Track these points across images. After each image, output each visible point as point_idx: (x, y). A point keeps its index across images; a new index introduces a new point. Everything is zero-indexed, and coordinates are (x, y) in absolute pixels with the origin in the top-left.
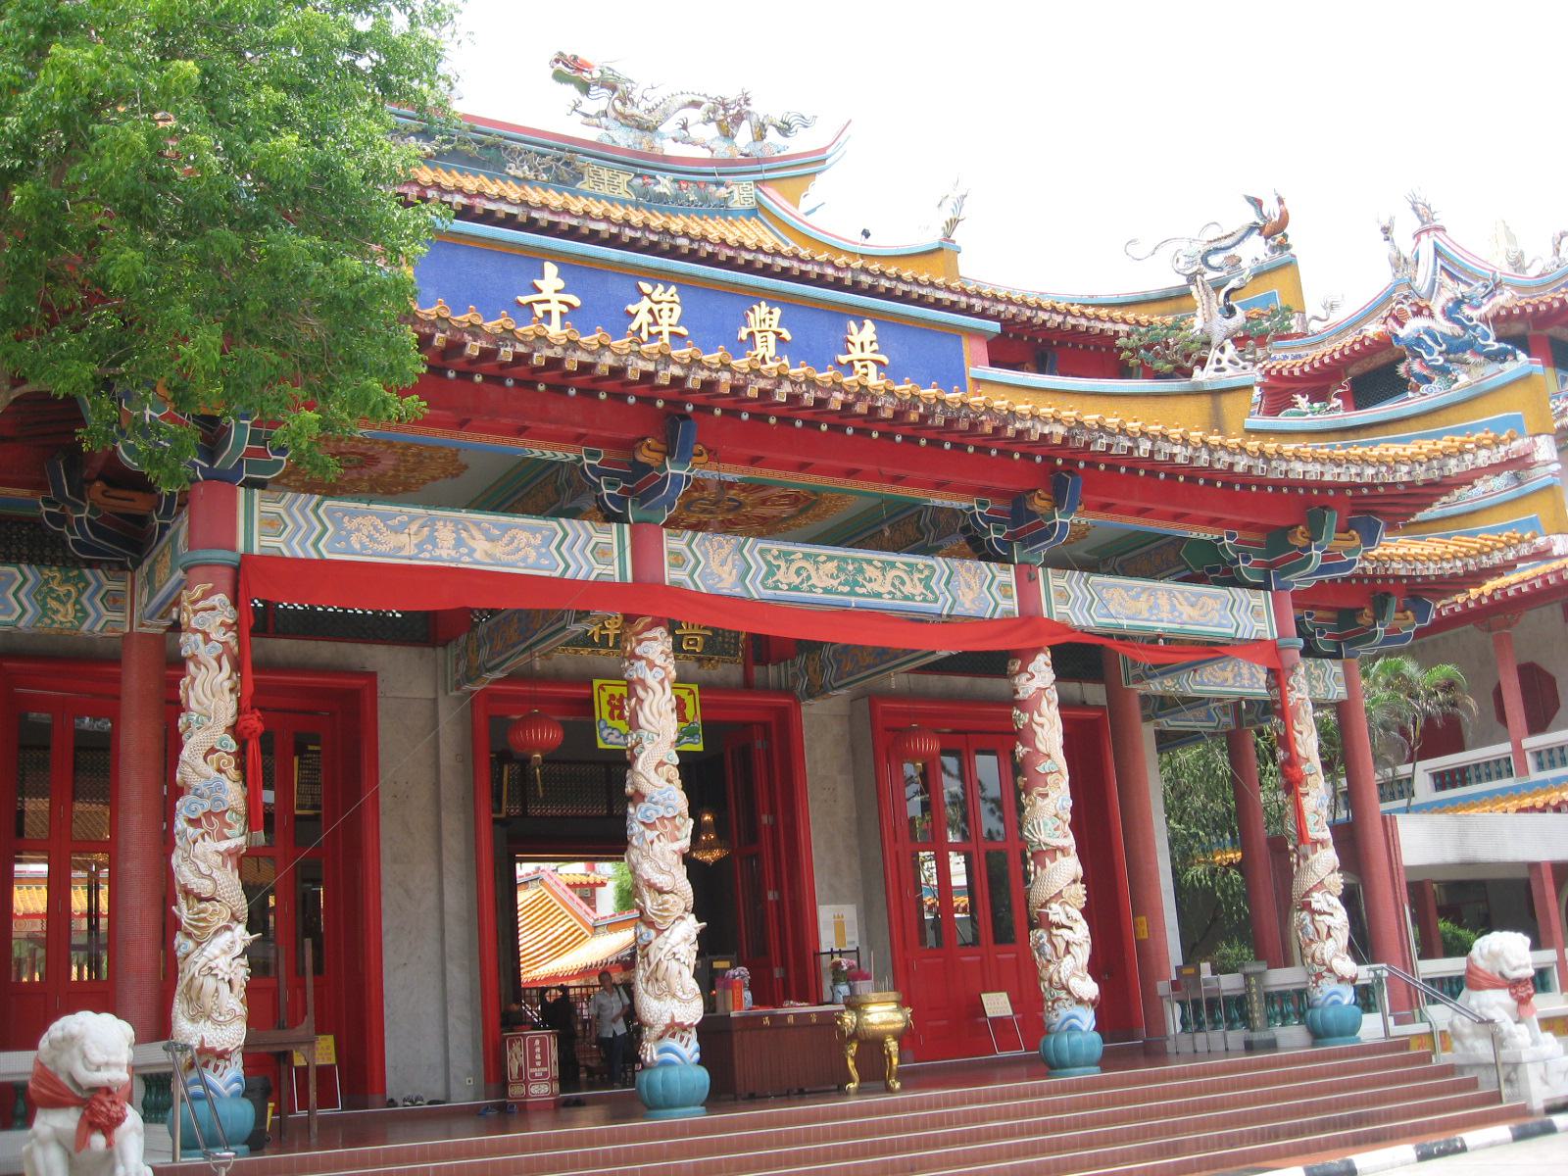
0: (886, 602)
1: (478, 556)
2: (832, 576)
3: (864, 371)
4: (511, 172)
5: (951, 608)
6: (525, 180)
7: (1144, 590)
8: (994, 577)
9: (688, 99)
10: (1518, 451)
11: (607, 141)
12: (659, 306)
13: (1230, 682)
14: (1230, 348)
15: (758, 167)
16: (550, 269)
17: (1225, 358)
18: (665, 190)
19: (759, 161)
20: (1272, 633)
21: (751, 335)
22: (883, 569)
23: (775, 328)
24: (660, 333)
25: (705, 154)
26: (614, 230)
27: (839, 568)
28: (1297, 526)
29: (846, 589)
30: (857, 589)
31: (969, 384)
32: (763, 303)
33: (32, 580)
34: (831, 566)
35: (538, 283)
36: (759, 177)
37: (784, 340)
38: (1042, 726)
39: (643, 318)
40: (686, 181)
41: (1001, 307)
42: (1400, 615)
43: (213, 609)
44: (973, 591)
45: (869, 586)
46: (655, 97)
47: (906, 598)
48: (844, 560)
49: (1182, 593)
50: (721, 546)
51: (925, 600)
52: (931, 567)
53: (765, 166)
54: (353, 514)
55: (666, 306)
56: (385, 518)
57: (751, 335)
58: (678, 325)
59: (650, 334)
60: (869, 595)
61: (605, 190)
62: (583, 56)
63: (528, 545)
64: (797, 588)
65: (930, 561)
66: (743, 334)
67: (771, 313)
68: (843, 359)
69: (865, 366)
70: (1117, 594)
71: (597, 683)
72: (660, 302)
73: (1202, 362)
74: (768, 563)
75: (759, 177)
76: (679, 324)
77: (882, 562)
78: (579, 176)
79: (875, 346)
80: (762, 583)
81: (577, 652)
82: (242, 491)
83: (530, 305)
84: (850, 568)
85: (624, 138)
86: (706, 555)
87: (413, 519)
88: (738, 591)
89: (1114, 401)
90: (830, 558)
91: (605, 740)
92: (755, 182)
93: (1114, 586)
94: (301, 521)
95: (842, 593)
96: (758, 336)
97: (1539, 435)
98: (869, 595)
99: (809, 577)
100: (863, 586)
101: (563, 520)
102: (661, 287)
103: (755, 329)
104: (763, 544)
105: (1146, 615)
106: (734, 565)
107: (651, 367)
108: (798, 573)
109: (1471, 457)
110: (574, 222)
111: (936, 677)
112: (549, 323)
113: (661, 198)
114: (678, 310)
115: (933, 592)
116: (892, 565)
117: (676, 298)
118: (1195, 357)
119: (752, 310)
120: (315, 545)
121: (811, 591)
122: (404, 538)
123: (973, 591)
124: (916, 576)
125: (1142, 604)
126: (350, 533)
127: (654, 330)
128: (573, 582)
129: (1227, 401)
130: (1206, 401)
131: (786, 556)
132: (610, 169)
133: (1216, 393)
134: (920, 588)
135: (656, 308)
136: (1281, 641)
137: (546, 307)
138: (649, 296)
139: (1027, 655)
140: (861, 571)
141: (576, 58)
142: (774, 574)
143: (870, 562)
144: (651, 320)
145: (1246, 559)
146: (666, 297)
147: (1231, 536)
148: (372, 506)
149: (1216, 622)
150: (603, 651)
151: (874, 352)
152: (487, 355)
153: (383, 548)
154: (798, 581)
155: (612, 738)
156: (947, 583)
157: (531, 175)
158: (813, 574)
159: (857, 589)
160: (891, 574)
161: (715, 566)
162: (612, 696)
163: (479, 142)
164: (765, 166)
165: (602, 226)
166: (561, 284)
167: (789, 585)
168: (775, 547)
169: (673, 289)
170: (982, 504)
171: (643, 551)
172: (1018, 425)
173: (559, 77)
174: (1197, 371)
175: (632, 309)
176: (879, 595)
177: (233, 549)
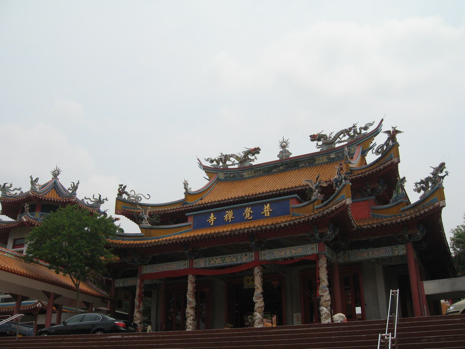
0: (229, 263)
2: (220, 261)
4: (300, 166)
5: (241, 262)
6: (303, 167)
7: (283, 250)
9: (341, 132)
10: (342, 204)
11: (322, 151)
13: (366, 256)
15: (357, 141)
16: (212, 214)
18: (334, 157)
19: (358, 139)
20: (316, 252)
21: (245, 214)
22: (229, 258)
25: (346, 143)
26: (234, 200)
27: (221, 259)
29: (222, 262)
30: (224, 262)
31: (291, 209)
34: (220, 259)
35: (210, 217)
36: (358, 143)
39: (227, 217)
40: (340, 152)
42: (413, 230)
45: (226, 261)
46: (333, 135)
47: (233, 262)
49: (293, 249)
50: (202, 260)
51: (236, 261)
52: (238, 255)
53: (359, 141)
55: (230, 214)
60: (226, 263)
61: (321, 162)
62: (316, 134)
64: (214, 264)
65: (237, 254)
66: (244, 215)
67: (249, 209)
68: (262, 213)
69: (267, 213)
70: (276, 252)
71: (244, 277)
74: (209, 261)
75: (358, 143)
78: (315, 161)
79: (269, 208)
80: (208, 264)
83: (209, 221)
85: (325, 148)
86: (200, 262)
88: (204, 266)
90: (220, 258)
91: (245, 287)
92: (357, 145)
93: (277, 250)
95: (221, 263)
96: (246, 214)
97: (346, 198)
98: (226, 263)
104: (209, 258)
105: (283, 255)
109: (331, 208)
110: (227, 201)
113: (333, 158)
114: (232, 214)
116: (230, 257)
117: (232, 212)
119: (246, 210)
125: (283, 253)
127: (228, 219)
128: (181, 270)
129: (316, 203)
131: (212, 259)
132: (321, 156)
134: (235, 260)
137: (211, 221)
139: (254, 268)
140: (225, 259)
141: (314, 135)
142: (210, 262)
143: (226, 257)
146: (231, 212)
148: (157, 265)
155: (246, 287)
157: (304, 165)
159: (224, 262)
160: (230, 258)
161: (201, 263)
162: (247, 279)
163: (294, 162)
164: (359, 141)
165: (232, 200)
168: (210, 258)
172: (221, 234)
173: (312, 140)
175: (224, 216)
176: (228, 262)
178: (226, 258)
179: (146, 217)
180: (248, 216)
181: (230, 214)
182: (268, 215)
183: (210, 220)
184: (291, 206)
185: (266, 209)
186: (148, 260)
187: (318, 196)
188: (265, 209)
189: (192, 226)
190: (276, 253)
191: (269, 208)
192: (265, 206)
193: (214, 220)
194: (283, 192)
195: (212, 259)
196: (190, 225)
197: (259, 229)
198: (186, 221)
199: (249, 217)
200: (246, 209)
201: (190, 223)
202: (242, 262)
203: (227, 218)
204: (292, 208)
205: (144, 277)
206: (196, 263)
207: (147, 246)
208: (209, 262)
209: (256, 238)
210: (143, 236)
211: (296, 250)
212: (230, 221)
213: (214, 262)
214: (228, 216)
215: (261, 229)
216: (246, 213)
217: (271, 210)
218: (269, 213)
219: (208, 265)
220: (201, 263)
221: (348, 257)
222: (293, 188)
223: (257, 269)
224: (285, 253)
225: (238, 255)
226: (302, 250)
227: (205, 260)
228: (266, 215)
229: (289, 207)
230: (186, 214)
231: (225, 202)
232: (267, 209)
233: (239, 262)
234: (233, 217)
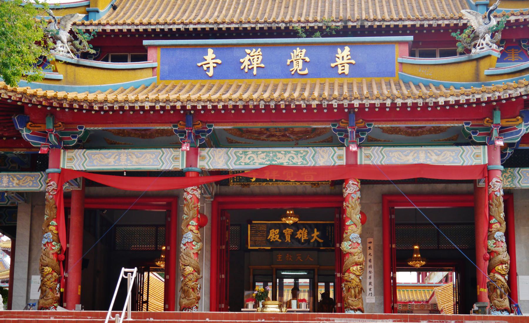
1: (134, 163)
2: (263, 159)
3: (343, 68)
7: (411, 151)
8: (335, 153)
12: (253, 58)
14: (488, 37)
16: (210, 51)
17: (484, 43)
21: (292, 62)
23: (302, 57)
24: (253, 68)
27: (267, 156)
28: (485, 118)
32: (298, 49)
33: (44, 176)
34: (263, 155)
35: (205, 57)
37: (306, 62)
38: (348, 207)
39: (247, 63)
41: (440, 22)
43: (51, 185)
44: (328, 157)
48: (269, 152)
49: (432, 151)
50: (219, 152)
54: (95, 154)
55: (256, 57)
56: (104, 154)
57: (292, 62)
58: (260, 64)
59: (248, 69)
63: (150, 158)
64: (248, 164)
65: (306, 149)
66: (288, 63)
68: (333, 65)
69: (344, 66)
70: (396, 154)
72: (254, 56)
73: (475, 46)
76: (262, 62)
77: (285, 152)
79: (349, 57)
80: (234, 163)
81: (260, 184)
82: (62, 151)
83: (202, 66)
84: (271, 155)
87: (113, 154)
88: (225, 167)
89: (441, 67)
90: (263, 152)
93: (396, 151)
94: (79, 158)
96: (295, 62)
99: (254, 160)
100: (276, 161)
101: (163, 149)
102: (254, 50)
103: (293, 59)
106: (224, 158)
107: (153, 104)
108: (249, 159)
110: (237, 26)
111: (426, 185)
112: (209, 72)
115: (306, 161)
116: (289, 152)
117: (261, 53)
118: (473, 43)
119: (293, 52)
120: (83, 165)
121: (254, 165)
122: (110, 160)
123: (328, 157)
124: (299, 155)
126: (93, 160)
127: (250, 67)
129: (483, 64)
130: (474, 63)
131: (245, 153)
133: (478, 60)
134: (301, 160)
135: (251, 58)
136: (491, 167)
137: (208, 66)
138: (249, 54)
140: (275, 156)
143: (279, 152)
144: (249, 63)
145: (474, 133)
146: (257, 53)
147: (466, 124)
149: (451, 161)
150: (271, 183)
151: (349, 59)
152: (101, 109)
153: (103, 164)
154: (249, 161)
156: (313, 157)
158: (255, 158)
160: (288, 156)
161: (216, 159)
166: (214, 56)
167: (245, 163)
168: (241, 150)
169: (259, 50)
170: (334, 125)
171: (192, 155)
174: (473, 51)
175: (242, 60)
177: (58, 168)
178: (279, 155)
179: (64, 35)
180: (298, 66)
181: (256, 57)
182: (347, 71)
183: (205, 64)
184: (400, 60)
185: (341, 58)
186: (75, 137)
187: (492, 49)
188: (338, 58)
189: (158, 70)
190: (394, 156)
191: (347, 56)
192: (339, 50)
193: (215, 65)
194: (371, 27)
195: (245, 153)
196: (153, 68)
197: (388, 102)
198: (144, 58)
199: (300, 70)
200: (295, 51)
201: (155, 64)
202: (317, 165)
203: (249, 65)
204: (399, 63)
205: (65, 175)
206: (203, 158)
207: (106, 107)
208: (236, 158)
209: (361, 120)
210: (60, 80)
211: (440, 155)
212: (255, 72)
213: (249, 159)
214: (249, 60)
215: (394, 105)
216: (293, 59)
217: (353, 62)
218: (347, 67)
219: (234, 165)
220: (216, 159)
221: (510, 179)
222: (395, 21)
223: (353, 184)
224: (415, 158)
225: (307, 152)
226: (453, 157)
227: (227, 153)
228: (340, 72)
229: (394, 62)
230: (145, 42)
231: (232, 26)
232: (343, 57)
233: (311, 164)
234: (262, 65)
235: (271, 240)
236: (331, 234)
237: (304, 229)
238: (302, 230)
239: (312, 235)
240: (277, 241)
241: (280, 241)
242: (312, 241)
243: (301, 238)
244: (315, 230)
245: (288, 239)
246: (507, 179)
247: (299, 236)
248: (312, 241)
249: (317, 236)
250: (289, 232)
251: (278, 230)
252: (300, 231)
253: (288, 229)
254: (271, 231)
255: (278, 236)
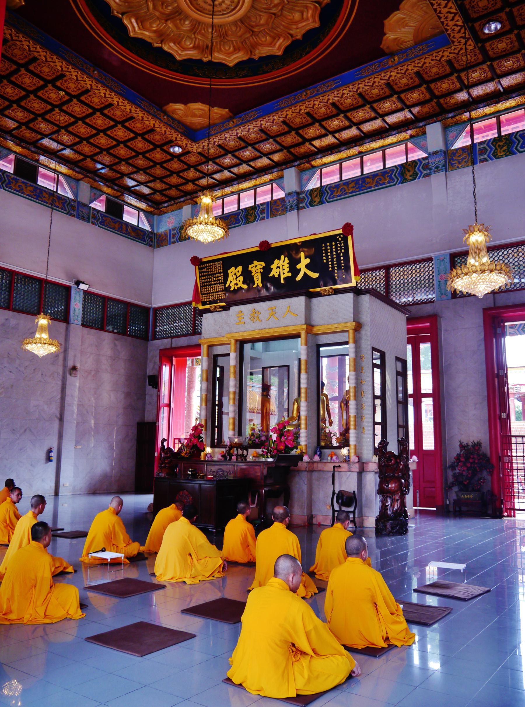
235: (232, 289)
236: (332, 258)
237: (282, 257)
238: (279, 259)
239: (298, 267)
240: (241, 288)
241: (245, 287)
242: (299, 278)
243: (279, 275)
244: (302, 255)
245: (258, 281)
246: (501, 149)
247: (274, 272)
248: (299, 278)
249: (307, 266)
250: (259, 267)
251: (240, 268)
252: (276, 261)
253: (255, 263)
254: (229, 271)
255: (241, 278)
